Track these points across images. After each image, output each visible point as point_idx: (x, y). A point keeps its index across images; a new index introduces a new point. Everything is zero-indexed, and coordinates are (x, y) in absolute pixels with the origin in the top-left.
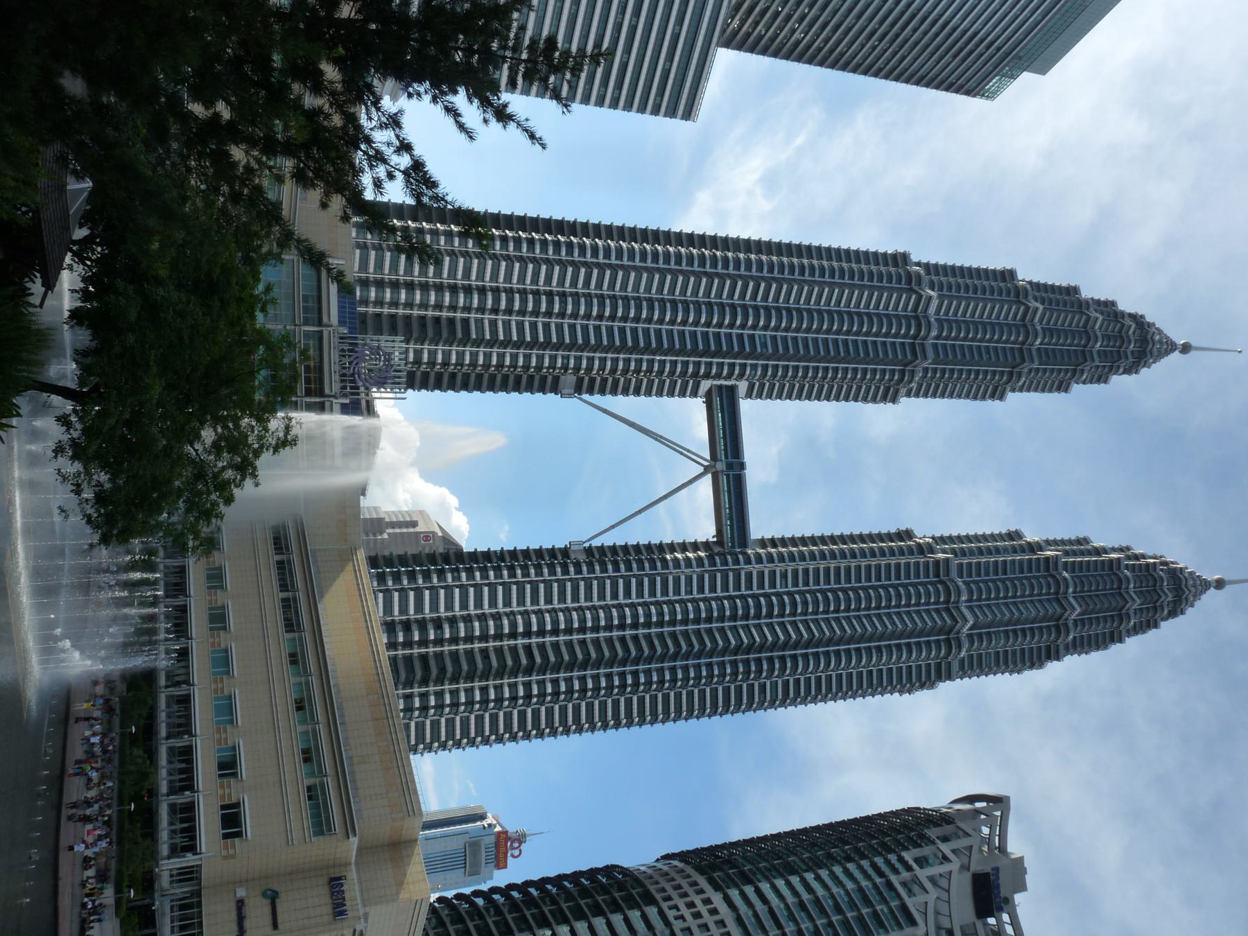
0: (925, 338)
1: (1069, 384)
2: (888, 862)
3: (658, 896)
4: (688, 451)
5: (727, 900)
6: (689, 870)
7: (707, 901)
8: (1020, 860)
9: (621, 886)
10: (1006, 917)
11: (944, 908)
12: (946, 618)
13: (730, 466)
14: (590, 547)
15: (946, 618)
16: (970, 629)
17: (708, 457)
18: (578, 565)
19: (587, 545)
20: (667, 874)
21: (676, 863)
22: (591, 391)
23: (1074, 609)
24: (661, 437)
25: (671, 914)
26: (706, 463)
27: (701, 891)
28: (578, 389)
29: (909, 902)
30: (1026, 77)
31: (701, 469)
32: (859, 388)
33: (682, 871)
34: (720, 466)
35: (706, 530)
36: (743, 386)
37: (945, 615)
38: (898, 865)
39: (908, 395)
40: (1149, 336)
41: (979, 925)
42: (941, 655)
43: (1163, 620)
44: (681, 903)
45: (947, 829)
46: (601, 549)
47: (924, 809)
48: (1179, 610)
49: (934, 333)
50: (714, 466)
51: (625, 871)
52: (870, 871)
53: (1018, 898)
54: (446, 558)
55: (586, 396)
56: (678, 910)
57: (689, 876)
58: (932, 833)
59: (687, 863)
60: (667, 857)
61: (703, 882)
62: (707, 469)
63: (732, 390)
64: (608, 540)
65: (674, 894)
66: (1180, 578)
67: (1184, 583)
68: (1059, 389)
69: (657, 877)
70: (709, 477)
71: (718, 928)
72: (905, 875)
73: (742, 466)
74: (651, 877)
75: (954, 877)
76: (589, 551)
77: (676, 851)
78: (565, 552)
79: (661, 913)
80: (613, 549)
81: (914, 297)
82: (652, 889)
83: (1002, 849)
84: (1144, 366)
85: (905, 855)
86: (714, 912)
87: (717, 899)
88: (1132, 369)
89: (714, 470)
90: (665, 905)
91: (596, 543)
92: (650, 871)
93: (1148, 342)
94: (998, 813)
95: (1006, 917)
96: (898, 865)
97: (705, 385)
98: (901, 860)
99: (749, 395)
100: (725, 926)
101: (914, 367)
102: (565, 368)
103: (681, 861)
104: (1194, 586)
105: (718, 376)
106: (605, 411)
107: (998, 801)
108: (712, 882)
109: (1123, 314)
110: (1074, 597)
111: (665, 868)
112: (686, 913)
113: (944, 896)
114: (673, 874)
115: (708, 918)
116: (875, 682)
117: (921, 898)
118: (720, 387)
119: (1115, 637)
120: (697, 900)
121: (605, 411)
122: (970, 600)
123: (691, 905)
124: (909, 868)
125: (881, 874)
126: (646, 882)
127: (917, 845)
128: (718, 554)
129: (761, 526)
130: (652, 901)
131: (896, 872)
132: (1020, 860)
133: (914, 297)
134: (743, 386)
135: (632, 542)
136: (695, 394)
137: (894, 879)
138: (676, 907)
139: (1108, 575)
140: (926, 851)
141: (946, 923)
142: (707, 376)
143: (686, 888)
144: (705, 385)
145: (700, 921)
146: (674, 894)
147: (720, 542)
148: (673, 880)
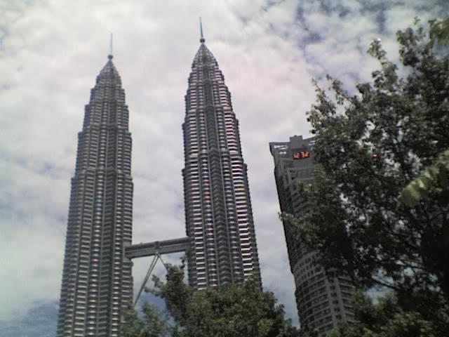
8: (291, 138)
13: (157, 248)
17: (152, 257)
26: (157, 257)
36: (126, 244)
62: (158, 257)
63: (127, 249)
70: (163, 256)
73: (157, 243)
99: (131, 241)
109: (96, 86)
127: (283, 183)
132: (291, 138)
136: (131, 264)
140: (284, 179)
144: (125, 260)
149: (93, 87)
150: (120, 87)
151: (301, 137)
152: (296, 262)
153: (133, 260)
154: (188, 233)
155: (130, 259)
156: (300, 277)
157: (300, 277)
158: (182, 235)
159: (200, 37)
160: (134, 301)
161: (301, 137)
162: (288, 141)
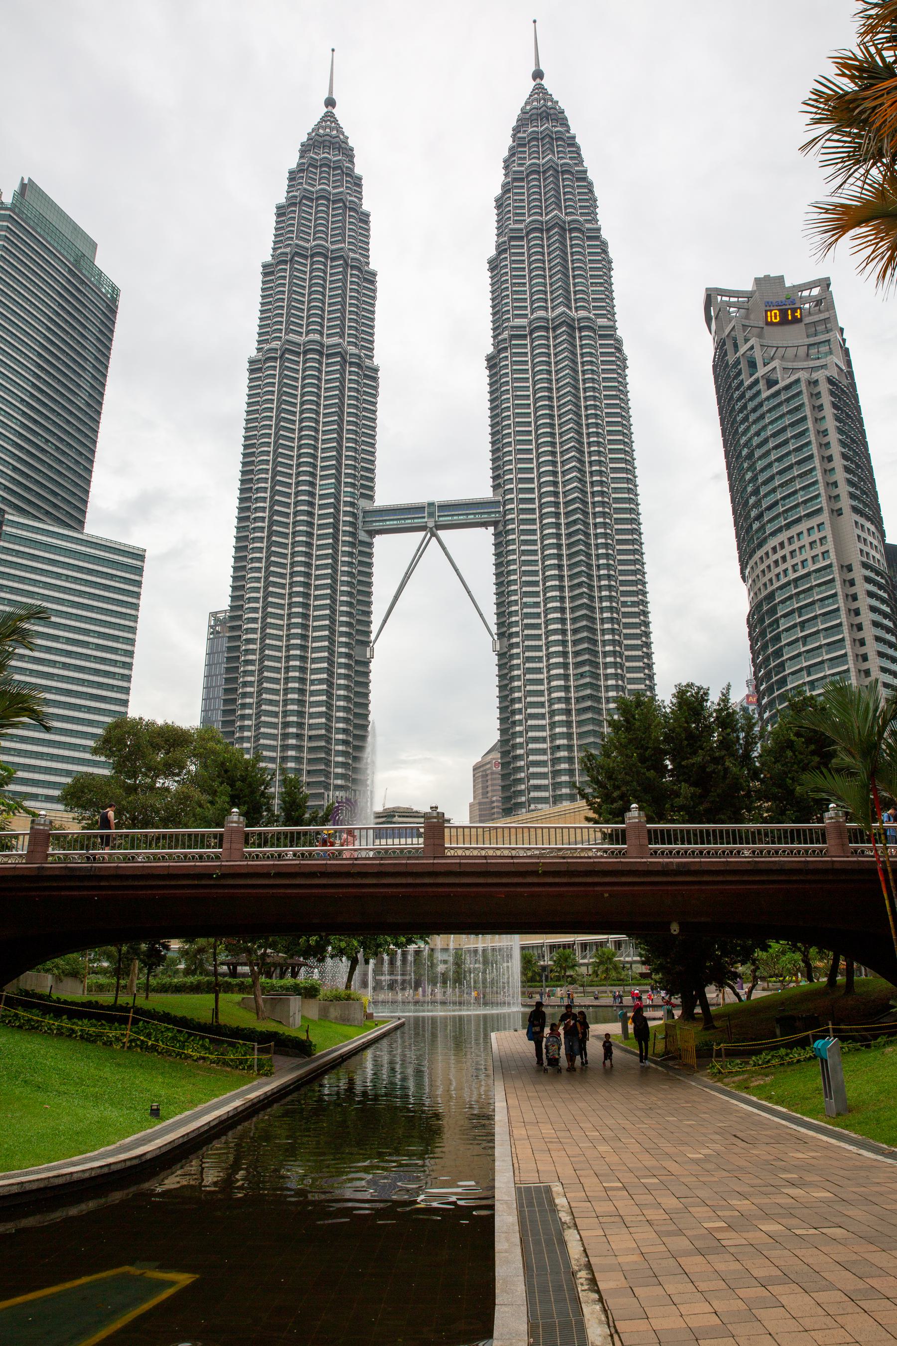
0: (322, 345)
1: (362, 213)
2: (752, 399)
3: (770, 589)
4: (418, 550)
5: (773, 534)
6: (751, 563)
7: (774, 550)
8: (758, 281)
9: (761, 620)
10: (806, 293)
11: (791, 352)
12: (561, 330)
13: (431, 515)
14: (498, 634)
15: (561, 330)
16: (570, 308)
17: (424, 533)
18: (512, 646)
19: (496, 637)
20: (754, 581)
21: (747, 572)
22: (368, 633)
23: (556, 216)
24: (406, 573)
25: (783, 580)
26: (429, 535)
27: (767, 554)
28: (366, 644)
29: (782, 384)
30: (101, 261)
31: (434, 539)
32: (365, 409)
33: (752, 568)
35: (486, 536)
37: (559, 332)
38: (754, 390)
39: (371, 357)
40: (320, 139)
41: (807, 320)
42: (593, 335)
43: (568, 132)
45: (729, 346)
46: (500, 625)
47: (714, 361)
48: (560, 116)
49: (317, 337)
50: (431, 528)
51: (751, 615)
52: (758, 414)
53: (788, 284)
54: (504, 754)
55: (373, 637)
56: (779, 574)
57: (756, 563)
58: (731, 359)
59: (747, 563)
60: (744, 578)
61: (760, 553)
62: (433, 535)
63: (366, 513)
64: (492, 620)
65: (768, 576)
66: (531, 115)
67: (534, 111)
68: (367, 222)
69: (756, 589)
70: (440, 533)
72: (762, 385)
73: (431, 505)
74: (756, 594)
75: (765, 342)
76: (501, 635)
77: (738, 568)
78: (501, 655)
79: (781, 588)
80: (499, 615)
81: (287, 356)
82: (764, 593)
83: (749, 295)
84: (346, 143)
85: (747, 383)
86: (782, 545)
87: (774, 542)
88: (349, 154)
89: (434, 529)
90: (776, 585)
91: (494, 629)
92: (752, 594)
93: (324, 141)
94: (719, 298)
95: (806, 293)
96: (754, 390)
97: (363, 536)
98: (750, 387)
99: (371, 498)
100: (793, 537)
101: (346, 353)
102: (348, 656)
103: (746, 567)
104: (538, 101)
106: (385, 621)
107: (710, 297)
108: (760, 545)
109: (299, 165)
110: (547, 214)
111: (750, 581)
112: (782, 567)
113: (781, 351)
114: (754, 576)
115: (788, 549)
116: (614, 393)
117: (779, 374)
119: (582, 176)
120: (774, 557)
121: (385, 621)
122: (546, 309)
123: (776, 563)
124: (756, 382)
125: (761, 405)
126: (760, 597)
128: (505, 526)
129: (484, 490)
130: (771, 596)
131: (758, 393)
132: (758, 281)
133: (287, 356)
134: (363, 503)
135: (494, 599)
136: (370, 545)
137: (765, 395)
138: (778, 575)
139: (528, 183)
140: (743, 365)
141: (802, 351)
142: (353, 534)
143: (763, 566)
144: (363, 536)
145: (788, 557)
146: (768, 576)
147: (495, 524)
148: (758, 576)
149: (293, 165)
150: (352, 170)
151: (781, 279)
152: (754, 552)
153: (378, 540)
154: (496, 487)
155: (372, 533)
156: (760, 584)
157: (760, 584)
158: (484, 490)
159: (533, 68)
160: (374, 628)
161: (781, 279)
162: (749, 286)
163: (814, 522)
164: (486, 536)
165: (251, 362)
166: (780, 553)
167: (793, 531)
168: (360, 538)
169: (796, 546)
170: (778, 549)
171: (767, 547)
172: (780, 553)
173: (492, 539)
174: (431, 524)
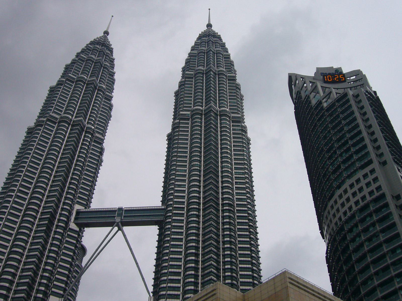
7: (340, 196)
13: (120, 215)
19: (151, 294)
31: (120, 232)
34: (118, 220)
35: (154, 230)
44: (342, 210)
50: (118, 223)
62: (120, 229)
70: (125, 229)
71: (357, 195)
73: (120, 209)
79: (347, 222)
91: (151, 289)
105: (68, 218)
118: (76, 219)
120: (340, 202)
123: (343, 205)
142: (67, 223)
163: (367, 170)
164: (154, 230)
165: (29, 129)
166: (345, 197)
167: (353, 180)
168: (70, 227)
169: (356, 188)
170: (343, 194)
171: (336, 196)
172: (345, 197)
173: (157, 232)
174: (118, 220)
